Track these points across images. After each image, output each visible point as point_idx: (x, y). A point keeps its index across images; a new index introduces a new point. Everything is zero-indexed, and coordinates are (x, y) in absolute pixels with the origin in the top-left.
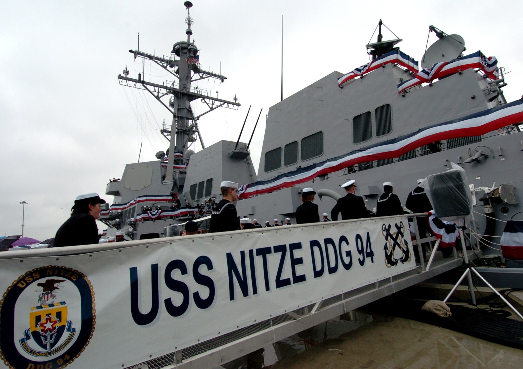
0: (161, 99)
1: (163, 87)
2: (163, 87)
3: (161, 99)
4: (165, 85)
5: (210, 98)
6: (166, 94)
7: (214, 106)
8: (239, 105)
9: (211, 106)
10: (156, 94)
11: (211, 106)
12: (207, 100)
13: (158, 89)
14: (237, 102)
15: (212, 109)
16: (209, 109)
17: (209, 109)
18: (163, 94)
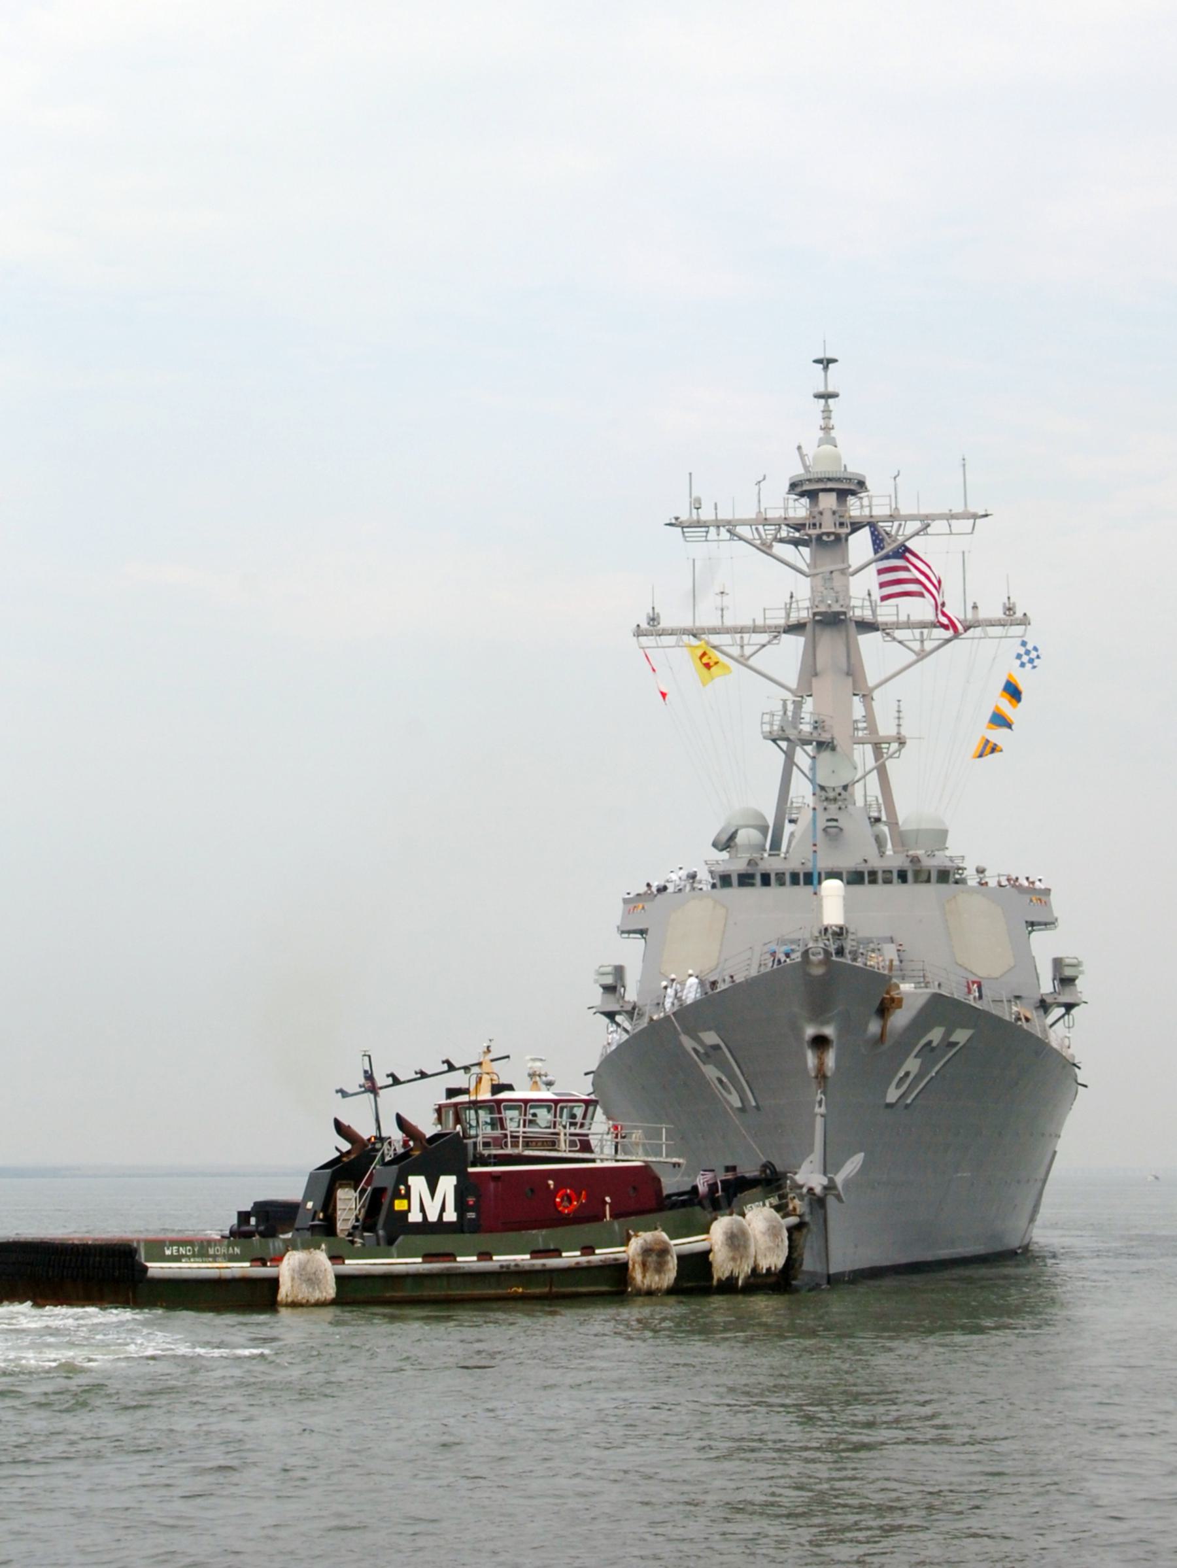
0: (751, 662)
1: (755, 630)
2: (755, 630)
3: (751, 662)
4: (760, 622)
5: (909, 625)
6: (769, 642)
7: (929, 646)
8: (1025, 621)
9: (916, 646)
10: (735, 651)
11: (916, 646)
12: (899, 634)
13: (742, 638)
14: (1019, 614)
15: (922, 655)
16: (914, 657)
17: (914, 657)
18: (758, 647)
